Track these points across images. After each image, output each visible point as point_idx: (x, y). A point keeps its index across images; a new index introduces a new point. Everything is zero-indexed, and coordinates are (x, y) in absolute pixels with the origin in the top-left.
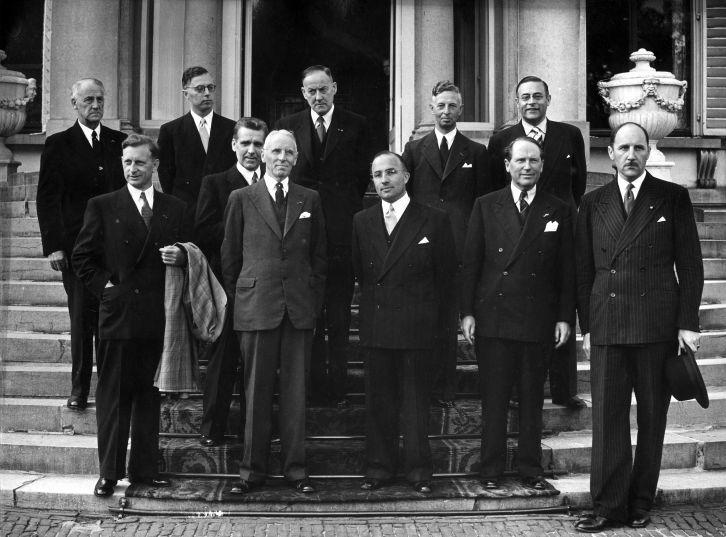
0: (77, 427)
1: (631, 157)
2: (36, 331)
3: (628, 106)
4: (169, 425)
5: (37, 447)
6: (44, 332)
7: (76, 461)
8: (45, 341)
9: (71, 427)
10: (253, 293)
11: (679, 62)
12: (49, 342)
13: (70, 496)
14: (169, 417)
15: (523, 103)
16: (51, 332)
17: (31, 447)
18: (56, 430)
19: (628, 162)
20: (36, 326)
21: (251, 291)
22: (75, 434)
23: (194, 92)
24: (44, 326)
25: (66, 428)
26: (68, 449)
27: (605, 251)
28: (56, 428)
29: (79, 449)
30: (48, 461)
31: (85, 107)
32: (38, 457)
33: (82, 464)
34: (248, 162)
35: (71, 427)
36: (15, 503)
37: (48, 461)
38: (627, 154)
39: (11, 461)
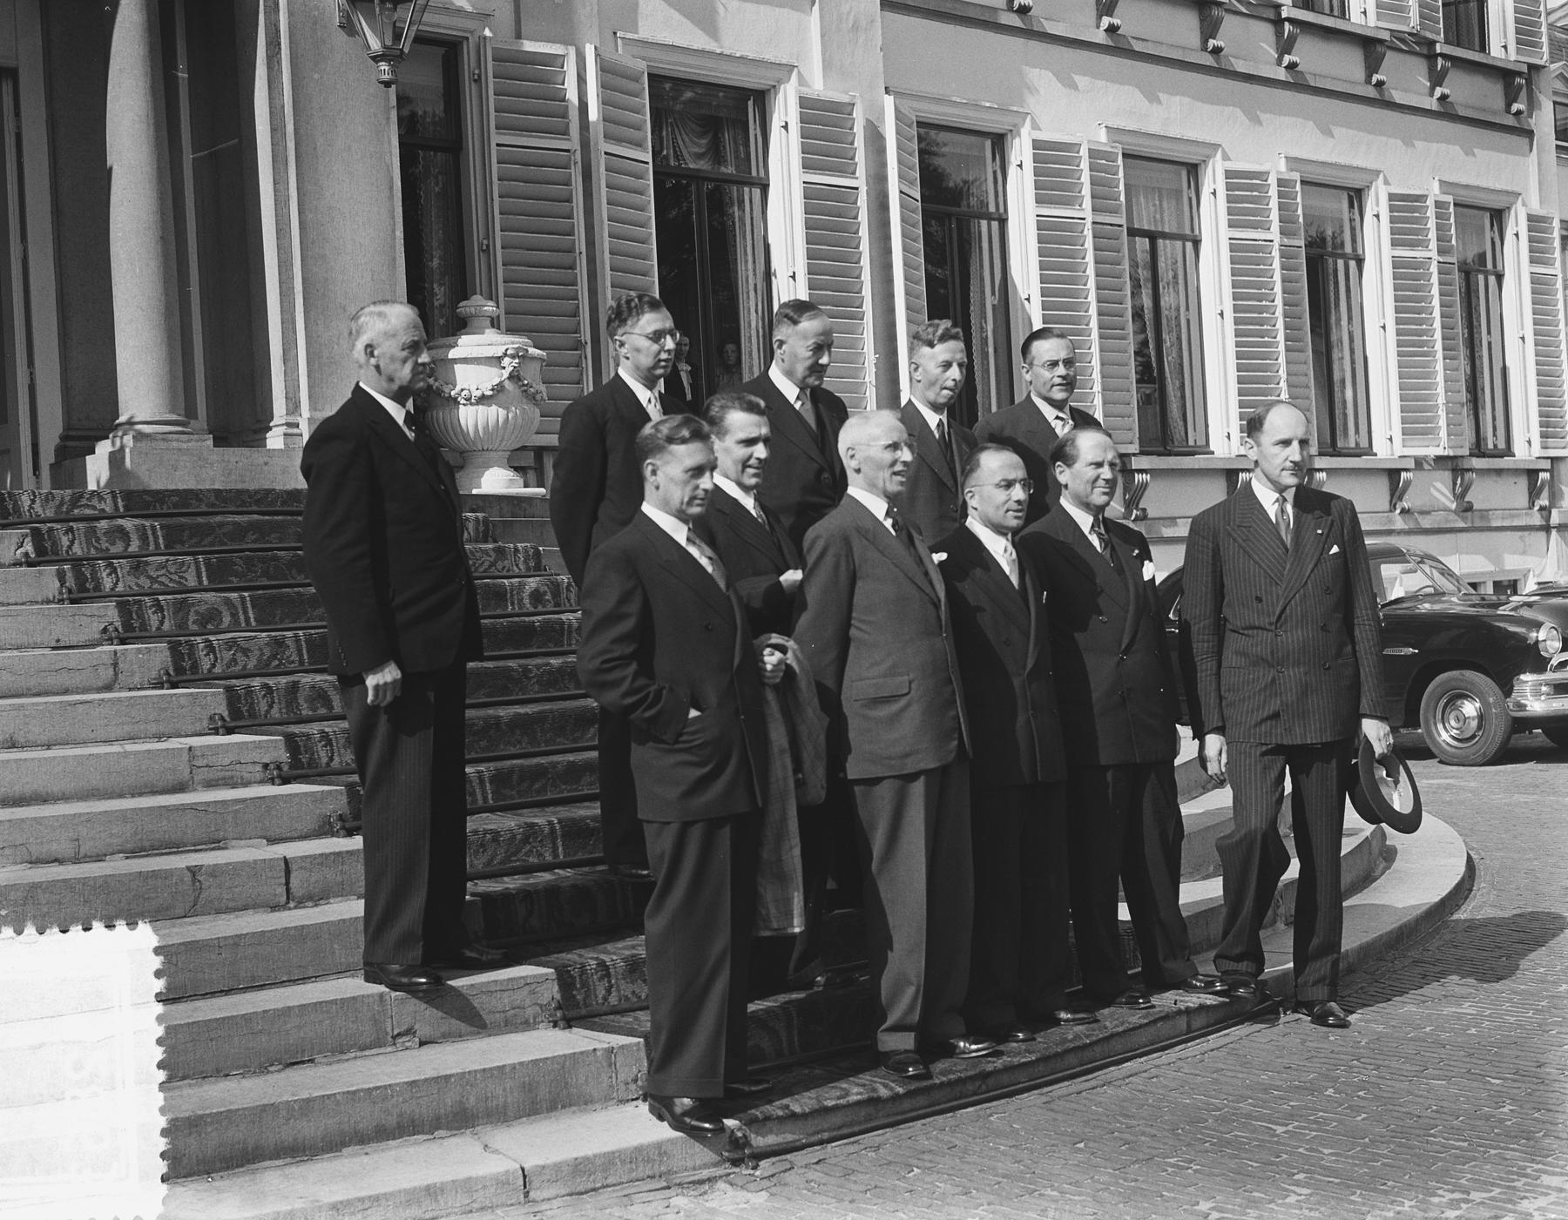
0: (423, 1031)
1: (1297, 458)
2: (36, 862)
3: (478, 394)
4: (609, 991)
5: (447, 1078)
6: (59, 861)
7: (529, 1088)
8: (154, 874)
9: (410, 1032)
10: (908, 705)
11: (442, 321)
12: (166, 875)
13: (639, 1149)
14: (608, 975)
15: (1047, 374)
16: (76, 860)
17: (436, 1079)
18: (378, 1043)
19: (1288, 464)
20: (36, 851)
21: (903, 702)
22: (422, 1044)
23: (645, 343)
24: (63, 847)
25: (399, 1035)
26: (513, 1067)
27: (1259, 600)
28: (380, 1040)
29: (535, 1062)
30: (472, 1099)
31: (404, 361)
32: (450, 1099)
33: (543, 1093)
34: (755, 475)
35: (410, 1032)
36: (526, 1194)
37: (472, 1099)
38: (1288, 450)
39: (392, 1121)
